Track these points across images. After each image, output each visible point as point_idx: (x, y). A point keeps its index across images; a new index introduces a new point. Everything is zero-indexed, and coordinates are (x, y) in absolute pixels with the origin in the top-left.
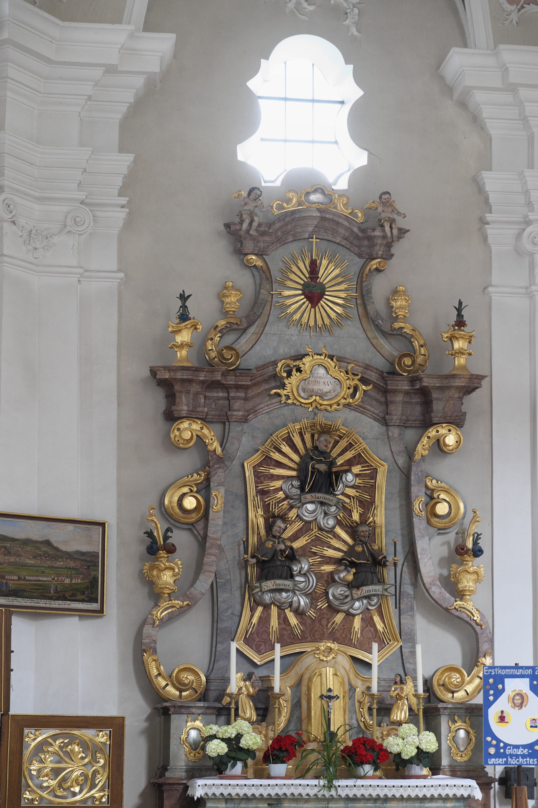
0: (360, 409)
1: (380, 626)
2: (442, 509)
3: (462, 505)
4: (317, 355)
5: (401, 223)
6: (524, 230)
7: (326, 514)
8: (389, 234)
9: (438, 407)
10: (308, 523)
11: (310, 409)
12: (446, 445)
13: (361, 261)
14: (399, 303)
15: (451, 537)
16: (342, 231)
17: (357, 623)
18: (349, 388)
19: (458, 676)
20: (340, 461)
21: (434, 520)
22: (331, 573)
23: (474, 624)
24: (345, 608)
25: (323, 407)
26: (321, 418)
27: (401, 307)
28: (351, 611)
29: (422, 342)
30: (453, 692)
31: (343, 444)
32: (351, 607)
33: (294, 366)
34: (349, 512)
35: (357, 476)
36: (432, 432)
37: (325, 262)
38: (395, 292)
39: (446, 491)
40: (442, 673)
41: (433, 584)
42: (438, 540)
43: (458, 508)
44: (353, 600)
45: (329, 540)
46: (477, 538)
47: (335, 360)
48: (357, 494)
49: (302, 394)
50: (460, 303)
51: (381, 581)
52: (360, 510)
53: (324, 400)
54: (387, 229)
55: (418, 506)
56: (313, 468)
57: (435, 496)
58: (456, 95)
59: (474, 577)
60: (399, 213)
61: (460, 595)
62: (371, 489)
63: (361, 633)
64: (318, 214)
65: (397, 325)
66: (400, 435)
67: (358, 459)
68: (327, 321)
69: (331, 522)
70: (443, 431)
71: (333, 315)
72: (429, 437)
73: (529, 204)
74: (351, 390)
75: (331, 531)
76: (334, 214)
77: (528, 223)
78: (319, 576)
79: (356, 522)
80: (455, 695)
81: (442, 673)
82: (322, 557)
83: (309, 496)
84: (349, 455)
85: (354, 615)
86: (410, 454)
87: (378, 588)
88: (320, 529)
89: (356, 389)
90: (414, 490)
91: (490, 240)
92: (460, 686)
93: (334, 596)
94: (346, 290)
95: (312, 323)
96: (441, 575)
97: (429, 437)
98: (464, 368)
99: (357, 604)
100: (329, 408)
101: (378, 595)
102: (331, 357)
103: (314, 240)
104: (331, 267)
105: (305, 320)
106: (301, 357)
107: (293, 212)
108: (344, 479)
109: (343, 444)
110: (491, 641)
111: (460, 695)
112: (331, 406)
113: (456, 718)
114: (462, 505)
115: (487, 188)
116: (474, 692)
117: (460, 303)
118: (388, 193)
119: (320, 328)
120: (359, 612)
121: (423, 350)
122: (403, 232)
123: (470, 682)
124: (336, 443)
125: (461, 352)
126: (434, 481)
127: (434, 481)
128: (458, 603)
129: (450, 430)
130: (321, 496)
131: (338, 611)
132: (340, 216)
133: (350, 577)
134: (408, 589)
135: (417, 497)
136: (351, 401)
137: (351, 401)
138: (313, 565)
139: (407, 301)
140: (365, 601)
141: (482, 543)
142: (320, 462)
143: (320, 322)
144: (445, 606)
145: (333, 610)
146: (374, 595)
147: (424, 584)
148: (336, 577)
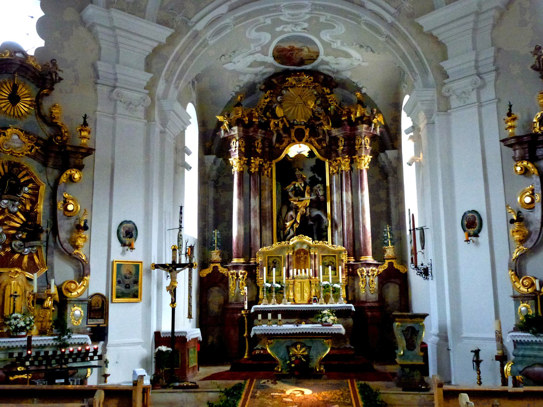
0: (34, 157)
1: (37, 261)
2: (70, 207)
3: (79, 207)
4: (15, 128)
5: (60, 74)
6: (114, 90)
7: (13, 205)
8: (54, 79)
9: (72, 161)
10: (4, 209)
11: (8, 155)
12: (74, 178)
13: (39, 89)
14: (56, 111)
15: (73, 220)
16: (30, 73)
17: (26, 259)
18: (29, 147)
19: (74, 285)
20: (22, 181)
21: (66, 212)
22: (14, 235)
23: (82, 260)
24: (20, 251)
25: (15, 154)
26: (14, 159)
27: (57, 113)
28: (23, 253)
29: (66, 130)
30: (71, 293)
31: (24, 172)
32: (23, 251)
33: (2, 133)
34: (25, 205)
35: (29, 188)
36: (68, 172)
37: (20, 87)
38: (54, 106)
39: (72, 200)
40: (68, 283)
41: (65, 242)
42: (67, 222)
43: (77, 208)
44: (25, 248)
45: (14, 218)
46: (86, 221)
47: (23, 132)
48: (30, 197)
49: (5, 147)
50: (86, 115)
51: (39, 239)
52: (31, 205)
53: (16, 151)
54: (54, 77)
55: (60, 205)
56: (9, 182)
57: (67, 201)
58: (87, 26)
59: (84, 240)
60: (60, 70)
61: (77, 247)
62: (36, 196)
63: (27, 264)
64: (20, 63)
65: (55, 121)
66: (52, 171)
67: (30, 181)
68: (20, 114)
69: (16, 209)
70: (73, 172)
71: (23, 112)
72: (67, 174)
73: (116, 80)
74: (30, 148)
75: (15, 214)
76: (28, 64)
77: (115, 87)
78: (8, 235)
79: (28, 210)
80: (73, 294)
81: (68, 283)
82: (9, 226)
83: (5, 196)
84: (26, 178)
85: (24, 255)
86: (57, 181)
87: (38, 243)
88: (10, 212)
89: (33, 147)
90: (58, 197)
91: (98, 92)
92: (75, 290)
93: (15, 245)
94: (30, 101)
95: (12, 113)
96: (67, 238)
97: (67, 174)
98: (84, 144)
99: (26, 250)
100: (17, 155)
101: (37, 246)
102: (22, 131)
103: (16, 75)
104: (24, 89)
105: (8, 111)
106: (6, 128)
107: (7, 59)
108: (23, 190)
109: (24, 172)
110: (89, 269)
111: (74, 294)
112: (19, 154)
113: (75, 305)
114: (79, 207)
115: (99, 68)
116: (81, 292)
117: (86, 115)
118: (55, 60)
119: (16, 117)
120: (27, 253)
121: (66, 134)
122: (61, 79)
123: (80, 288)
124: (21, 172)
125: (84, 137)
126: (67, 195)
127: (67, 195)
128: (76, 251)
129: (76, 172)
130: (12, 197)
131: (16, 253)
132: (31, 65)
133: (24, 237)
134: (51, 243)
135: (59, 201)
136: (29, 153)
137: (29, 153)
138: (5, 230)
139: (60, 111)
140: (30, 249)
141: (88, 224)
142: (12, 180)
143: (16, 114)
144: (69, 252)
145: (14, 252)
146: (35, 246)
147: (60, 241)
148: (17, 236)
